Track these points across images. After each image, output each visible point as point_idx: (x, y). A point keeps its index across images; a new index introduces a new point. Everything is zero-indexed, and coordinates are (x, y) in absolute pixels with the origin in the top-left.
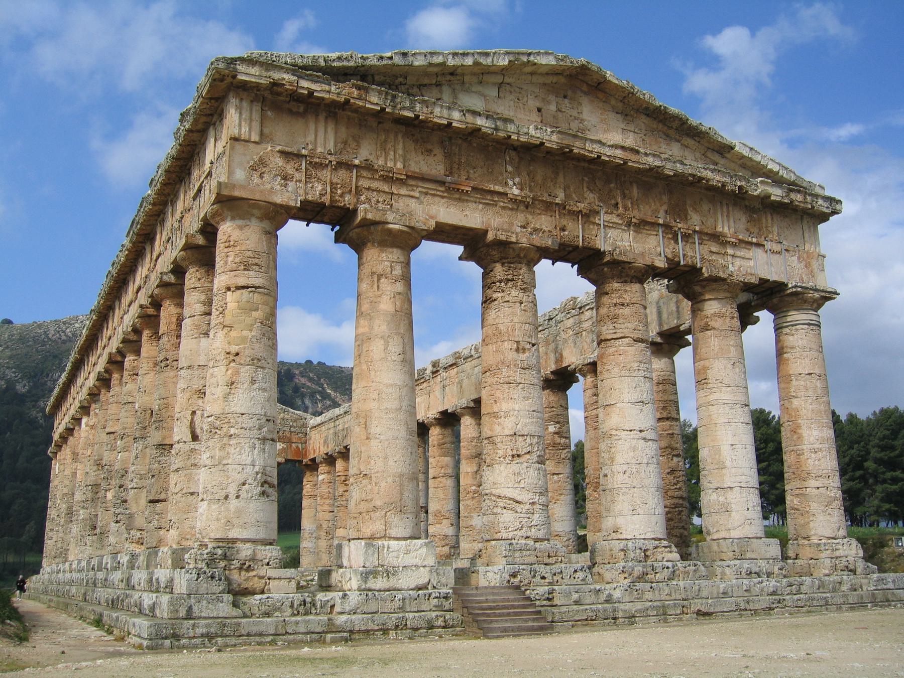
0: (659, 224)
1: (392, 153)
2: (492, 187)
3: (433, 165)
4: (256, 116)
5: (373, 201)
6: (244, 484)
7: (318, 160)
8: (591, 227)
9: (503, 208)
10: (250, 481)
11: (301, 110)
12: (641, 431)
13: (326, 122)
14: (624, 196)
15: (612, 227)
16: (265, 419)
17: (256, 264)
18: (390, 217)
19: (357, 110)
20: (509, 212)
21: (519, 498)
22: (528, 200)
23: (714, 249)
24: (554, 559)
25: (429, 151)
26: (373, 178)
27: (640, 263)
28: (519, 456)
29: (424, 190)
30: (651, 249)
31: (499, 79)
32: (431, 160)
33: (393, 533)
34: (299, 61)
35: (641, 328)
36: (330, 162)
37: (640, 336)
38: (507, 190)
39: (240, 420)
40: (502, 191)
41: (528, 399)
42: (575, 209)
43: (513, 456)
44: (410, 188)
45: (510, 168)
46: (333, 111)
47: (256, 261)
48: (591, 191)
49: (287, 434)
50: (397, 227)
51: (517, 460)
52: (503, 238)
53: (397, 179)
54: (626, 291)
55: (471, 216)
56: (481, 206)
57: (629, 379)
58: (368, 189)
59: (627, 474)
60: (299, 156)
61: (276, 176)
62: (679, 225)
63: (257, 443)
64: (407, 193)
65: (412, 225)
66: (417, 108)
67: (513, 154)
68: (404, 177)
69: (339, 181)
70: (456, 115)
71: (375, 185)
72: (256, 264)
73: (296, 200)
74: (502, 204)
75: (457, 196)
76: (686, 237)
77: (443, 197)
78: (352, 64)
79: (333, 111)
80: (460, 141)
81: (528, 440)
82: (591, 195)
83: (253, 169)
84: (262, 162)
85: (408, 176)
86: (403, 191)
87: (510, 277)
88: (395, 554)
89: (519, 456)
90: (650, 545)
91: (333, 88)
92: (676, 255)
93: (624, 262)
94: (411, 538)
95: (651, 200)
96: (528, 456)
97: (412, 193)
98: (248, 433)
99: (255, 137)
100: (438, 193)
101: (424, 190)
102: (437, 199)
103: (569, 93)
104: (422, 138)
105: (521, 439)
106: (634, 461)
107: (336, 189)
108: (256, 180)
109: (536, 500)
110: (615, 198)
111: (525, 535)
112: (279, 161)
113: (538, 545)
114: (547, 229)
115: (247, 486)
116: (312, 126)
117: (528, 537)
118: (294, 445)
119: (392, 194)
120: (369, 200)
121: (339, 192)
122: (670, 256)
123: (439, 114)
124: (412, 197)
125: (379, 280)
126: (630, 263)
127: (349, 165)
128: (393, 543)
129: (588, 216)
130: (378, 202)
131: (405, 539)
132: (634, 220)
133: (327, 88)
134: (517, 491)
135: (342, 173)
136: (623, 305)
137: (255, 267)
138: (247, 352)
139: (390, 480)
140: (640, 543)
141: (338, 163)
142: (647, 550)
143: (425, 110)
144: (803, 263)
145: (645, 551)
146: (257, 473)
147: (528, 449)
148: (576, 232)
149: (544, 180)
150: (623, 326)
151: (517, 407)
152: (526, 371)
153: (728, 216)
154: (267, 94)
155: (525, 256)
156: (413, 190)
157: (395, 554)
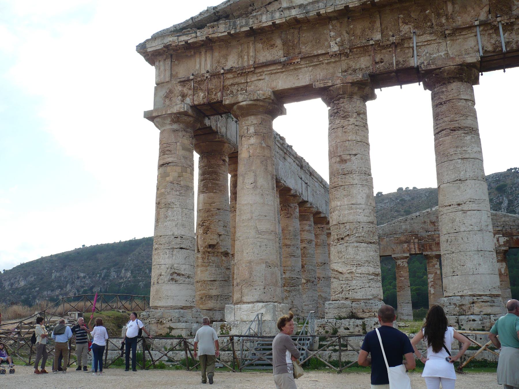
0: (476, 26)
1: (246, 57)
2: (315, 53)
3: (277, 53)
4: (168, 67)
5: (235, 91)
6: (161, 275)
7: (199, 79)
8: (407, 51)
9: (328, 64)
10: (163, 274)
11: (193, 52)
12: (459, 205)
13: (205, 54)
14: (439, 15)
15: (428, 44)
16: (173, 237)
17: (168, 150)
18: (240, 98)
19: (220, 39)
20: (333, 65)
21: (340, 270)
22: (346, 51)
24: (368, 314)
25: (273, 46)
26: (234, 77)
27: (451, 65)
28: (342, 239)
29: (268, 73)
30: (470, 48)
32: (274, 51)
33: (245, 299)
34: (178, 28)
35: (456, 119)
36: (207, 77)
37: (457, 125)
38: (329, 50)
39: (159, 239)
40: (324, 52)
41: (347, 196)
42: (388, 43)
43: (338, 239)
44: (259, 75)
45: (332, 34)
46: (208, 45)
47: (168, 148)
48: (407, 24)
49: (509, 230)
50: (244, 103)
51: (342, 242)
52: (322, 86)
53: (248, 72)
54: (443, 92)
55: (303, 78)
56: (311, 68)
57: (446, 164)
59: (449, 243)
60: (189, 80)
61: (178, 97)
62: (499, 19)
63: (167, 251)
64: (256, 78)
65: (255, 98)
66: (251, 23)
67: (334, 22)
68: (252, 69)
69: (213, 87)
70: (277, 15)
71: (237, 80)
72: (168, 150)
73: (184, 107)
74: (326, 61)
75: (292, 68)
76: (508, 27)
77: (282, 72)
78: (208, 14)
79: (208, 45)
81: (348, 227)
82: (407, 27)
83: (166, 97)
84: (171, 91)
85: (255, 68)
86: (254, 78)
87: (336, 111)
88: (245, 313)
89: (342, 239)
90: (467, 301)
91: (198, 34)
92: (497, 46)
93: (435, 69)
94: (258, 302)
95: (469, 9)
96: (347, 238)
97: (260, 78)
98: (162, 247)
100: (279, 71)
101: (268, 73)
102: (277, 75)
104: (267, 39)
105: (342, 226)
106: (452, 231)
107: (212, 92)
108: (167, 102)
109: (353, 270)
110: (430, 20)
111: (344, 297)
112: (180, 88)
113: (354, 304)
114: (363, 66)
115: (162, 276)
116: (198, 60)
117: (347, 298)
118: (515, 238)
119: (247, 82)
120: (232, 92)
121: (214, 92)
122: (490, 48)
123: (265, 20)
124: (260, 80)
125: (241, 139)
126: (440, 68)
127: (219, 75)
128: (245, 306)
129: (400, 44)
130: (238, 91)
131: (253, 302)
132: (447, 32)
133: (194, 35)
134: (340, 265)
135: (215, 81)
136: (441, 104)
137: (167, 152)
138: (163, 201)
139: (244, 265)
140: (457, 300)
141: (211, 76)
142: (463, 305)
143: (256, 22)
145: (461, 306)
146: (168, 268)
147: (347, 233)
148: (392, 60)
149: (364, 31)
150: (441, 121)
151: (339, 204)
152: (347, 177)
154: (172, 52)
155: (344, 93)
156: (261, 75)
157: (245, 313)
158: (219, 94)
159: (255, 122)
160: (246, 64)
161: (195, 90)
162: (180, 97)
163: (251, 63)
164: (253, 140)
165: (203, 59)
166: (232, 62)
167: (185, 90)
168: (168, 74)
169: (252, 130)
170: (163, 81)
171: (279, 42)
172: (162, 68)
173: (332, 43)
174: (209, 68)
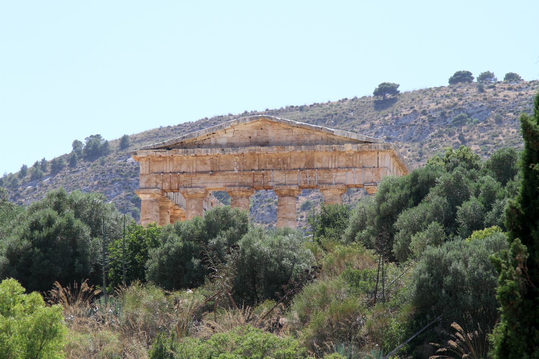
4: (147, 166)
23: (325, 177)
25: (206, 164)
31: (232, 130)
32: (206, 166)
58: (184, 181)
67: (237, 157)
75: (215, 177)
80: (216, 158)
82: (270, 166)
91: (167, 152)
99: (147, 173)
103: (263, 127)
116: (165, 165)
144: (375, 174)
153: (335, 161)
158: (177, 185)
159: (195, 202)
160: (191, 171)
161: (163, 181)
162: (155, 184)
163: (194, 171)
164: (194, 212)
165: (168, 165)
166: (184, 168)
167: (158, 181)
168: (148, 170)
169: (193, 207)
170: (145, 173)
171: (209, 162)
172: (144, 166)
173: (235, 168)
174: (171, 170)
